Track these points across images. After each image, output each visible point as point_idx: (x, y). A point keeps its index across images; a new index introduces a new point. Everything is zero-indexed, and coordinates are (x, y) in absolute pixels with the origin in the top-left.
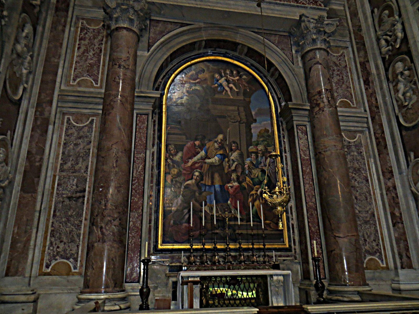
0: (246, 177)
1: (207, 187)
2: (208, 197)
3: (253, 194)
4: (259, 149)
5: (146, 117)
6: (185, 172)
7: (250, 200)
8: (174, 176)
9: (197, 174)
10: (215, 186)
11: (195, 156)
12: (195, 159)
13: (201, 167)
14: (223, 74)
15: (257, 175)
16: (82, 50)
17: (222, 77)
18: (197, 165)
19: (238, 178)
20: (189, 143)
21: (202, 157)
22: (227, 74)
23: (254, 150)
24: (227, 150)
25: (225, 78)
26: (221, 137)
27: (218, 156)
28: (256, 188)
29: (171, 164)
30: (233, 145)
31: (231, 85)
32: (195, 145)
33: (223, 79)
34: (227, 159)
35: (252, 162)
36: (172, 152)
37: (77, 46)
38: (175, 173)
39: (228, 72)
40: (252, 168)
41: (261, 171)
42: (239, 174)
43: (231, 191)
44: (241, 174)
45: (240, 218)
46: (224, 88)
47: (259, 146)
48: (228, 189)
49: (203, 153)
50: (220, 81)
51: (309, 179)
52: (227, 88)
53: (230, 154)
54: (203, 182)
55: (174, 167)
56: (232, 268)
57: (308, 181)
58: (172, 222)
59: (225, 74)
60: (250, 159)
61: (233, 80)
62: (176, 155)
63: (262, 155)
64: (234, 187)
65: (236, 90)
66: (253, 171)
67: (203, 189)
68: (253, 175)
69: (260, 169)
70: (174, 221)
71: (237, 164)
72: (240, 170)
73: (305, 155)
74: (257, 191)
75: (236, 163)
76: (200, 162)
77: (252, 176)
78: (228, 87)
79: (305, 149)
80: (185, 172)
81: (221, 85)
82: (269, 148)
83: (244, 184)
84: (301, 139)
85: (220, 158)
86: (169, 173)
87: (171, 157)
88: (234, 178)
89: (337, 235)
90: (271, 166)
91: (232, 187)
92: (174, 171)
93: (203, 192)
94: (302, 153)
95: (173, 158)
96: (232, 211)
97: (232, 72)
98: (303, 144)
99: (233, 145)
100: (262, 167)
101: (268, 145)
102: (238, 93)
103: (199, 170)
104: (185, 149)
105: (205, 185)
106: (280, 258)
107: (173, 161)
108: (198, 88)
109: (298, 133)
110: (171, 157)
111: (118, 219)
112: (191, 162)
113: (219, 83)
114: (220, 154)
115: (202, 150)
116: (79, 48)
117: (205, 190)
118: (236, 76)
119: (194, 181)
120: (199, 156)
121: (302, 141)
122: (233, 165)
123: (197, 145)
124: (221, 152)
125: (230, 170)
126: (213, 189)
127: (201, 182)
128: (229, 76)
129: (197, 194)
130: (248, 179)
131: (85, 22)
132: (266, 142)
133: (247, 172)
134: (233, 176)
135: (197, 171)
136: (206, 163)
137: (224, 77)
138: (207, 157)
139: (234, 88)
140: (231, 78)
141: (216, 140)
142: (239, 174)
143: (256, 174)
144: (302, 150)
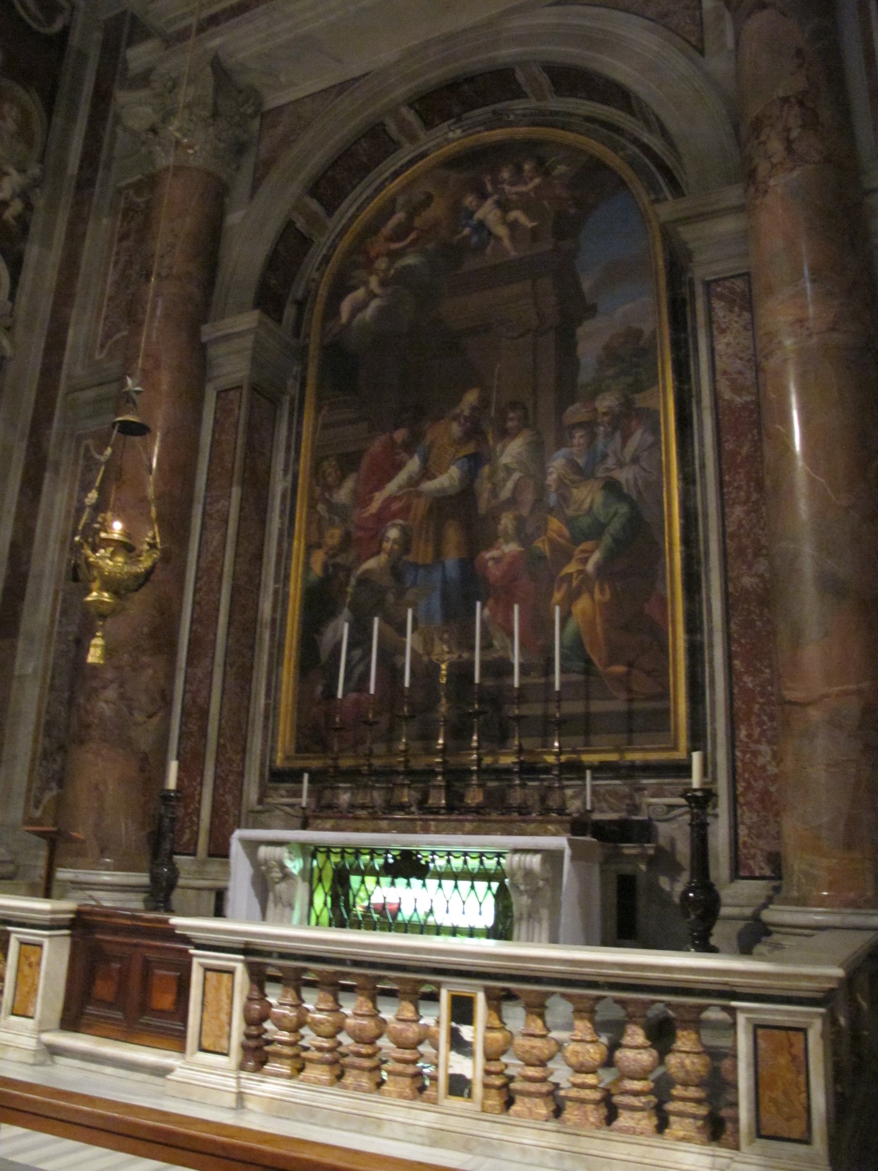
0: (549, 516)
5: (238, 394)
6: (361, 534)
7: (558, 596)
9: (393, 533)
10: (443, 566)
11: (390, 478)
12: (392, 487)
13: (405, 512)
14: (489, 188)
15: (586, 505)
16: (120, 266)
17: (483, 196)
18: (395, 506)
19: (520, 522)
21: (410, 478)
22: (503, 182)
25: (496, 197)
26: (471, 397)
27: (459, 463)
28: (583, 551)
29: (326, 515)
30: (511, 415)
33: (489, 203)
34: (486, 470)
35: (571, 463)
36: (330, 479)
37: (113, 259)
40: (573, 482)
42: (525, 511)
43: (494, 571)
44: (532, 512)
45: (521, 665)
46: (490, 233)
47: (600, 397)
49: (413, 465)
50: (479, 215)
52: (501, 231)
53: (498, 449)
54: (410, 558)
55: (332, 524)
56: (436, 827)
57: (742, 494)
58: (319, 689)
59: (496, 182)
60: (564, 451)
65: (530, 224)
66: (575, 491)
67: (409, 578)
71: (521, 478)
72: (528, 497)
73: (737, 389)
74: (585, 561)
75: (516, 476)
77: (570, 512)
79: (739, 365)
80: (361, 534)
81: (481, 226)
82: (637, 396)
84: (723, 331)
85: (466, 468)
86: (319, 546)
87: (327, 495)
88: (506, 528)
89: (790, 695)
92: (332, 537)
93: (407, 589)
95: (331, 496)
96: (496, 643)
97: (519, 169)
98: (730, 351)
100: (608, 470)
101: (638, 387)
102: (535, 235)
103: (400, 522)
104: (365, 462)
105: (416, 566)
107: (332, 507)
108: (410, 260)
109: (710, 310)
110: (327, 495)
111: (115, 686)
112: (379, 498)
113: (474, 221)
114: (465, 456)
115: (411, 456)
116: (116, 263)
117: (414, 584)
118: (531, 179)
119: (383, 558)
120: (402, 477)
121: (728, 338)
122: (505, 480)
124: (470, 448)
126: (437, 575)
127: (405, 558)
128: (507, 188)
129: (390, 598)
130: (555, 524)
131: (131, 192)
135: (394, 525)
136: (419, 494)
137: (491, 195)
138: (426, 473)
141: (457, 411)
142: (525, 511)
143: (583, 501)
144: (725, 373)
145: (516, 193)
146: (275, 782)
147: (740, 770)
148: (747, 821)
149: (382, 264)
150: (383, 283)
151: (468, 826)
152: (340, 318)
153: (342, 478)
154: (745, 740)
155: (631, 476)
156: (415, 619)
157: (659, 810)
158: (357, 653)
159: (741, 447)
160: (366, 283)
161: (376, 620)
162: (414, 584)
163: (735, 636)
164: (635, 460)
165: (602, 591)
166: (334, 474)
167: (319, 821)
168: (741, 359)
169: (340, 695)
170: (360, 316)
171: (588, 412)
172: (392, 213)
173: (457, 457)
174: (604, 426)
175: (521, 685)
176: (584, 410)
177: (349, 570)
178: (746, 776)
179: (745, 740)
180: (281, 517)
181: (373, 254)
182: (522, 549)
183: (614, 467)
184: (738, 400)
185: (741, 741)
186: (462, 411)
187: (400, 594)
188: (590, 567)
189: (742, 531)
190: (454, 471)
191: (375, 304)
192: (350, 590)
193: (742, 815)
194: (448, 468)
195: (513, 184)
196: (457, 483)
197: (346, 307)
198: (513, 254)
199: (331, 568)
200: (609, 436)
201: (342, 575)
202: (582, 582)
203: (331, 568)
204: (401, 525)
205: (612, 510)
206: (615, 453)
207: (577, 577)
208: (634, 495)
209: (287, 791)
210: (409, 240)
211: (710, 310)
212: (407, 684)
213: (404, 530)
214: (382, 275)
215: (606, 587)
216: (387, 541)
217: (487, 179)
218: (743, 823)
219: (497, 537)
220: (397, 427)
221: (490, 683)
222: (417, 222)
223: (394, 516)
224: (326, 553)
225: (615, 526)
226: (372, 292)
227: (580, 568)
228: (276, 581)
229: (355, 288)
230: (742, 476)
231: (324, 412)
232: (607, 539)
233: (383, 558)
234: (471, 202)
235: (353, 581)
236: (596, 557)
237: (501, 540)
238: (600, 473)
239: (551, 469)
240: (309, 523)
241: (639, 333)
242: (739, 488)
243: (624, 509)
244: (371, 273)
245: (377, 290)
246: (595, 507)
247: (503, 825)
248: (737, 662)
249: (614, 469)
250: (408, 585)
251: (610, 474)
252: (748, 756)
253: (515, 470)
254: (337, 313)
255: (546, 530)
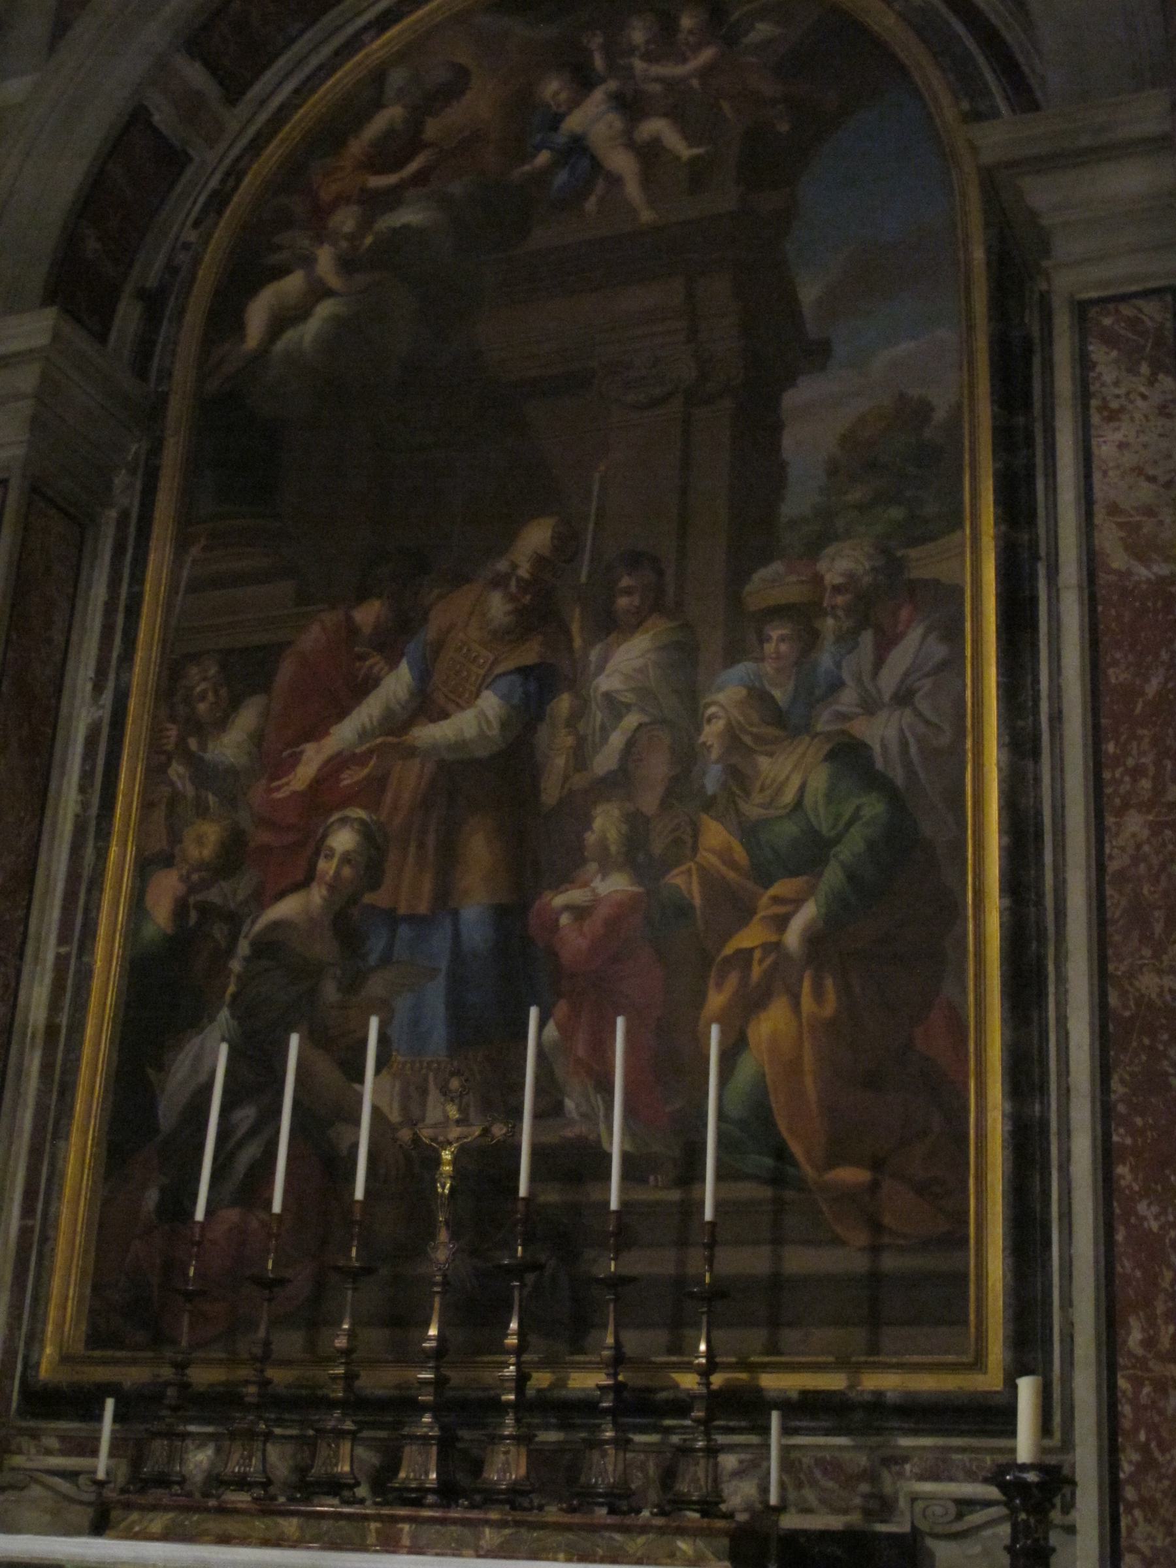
0: (704, 817)
1: (404, 931)
2: (403, 1004)
3: (751, 951)
4: (832, 578)
7: (716, 1000)
8: (195, 877)
9: (343, 840)
11: (342, 714)
14: (599, 62)
15: (789, 796)
17: (584, 81)
18: (349, 779)
20: (315, 630)
22: (632, 50)
23: (791, 591)
24: (575, 628)
25: (612, 85)
27: (503, 684)
28: (776, 900)
29: (190, 791)
30: (625, 582)
31: (656, 127)
32: (353, 630)
33: (598, 94)
34: (564, 703)
35: (758, 696)
36: (202, 707)
38: (207, 853)
39: (638, 34)
40: (757, 738)
41: (831, 756)
45: (626, 1157)
46: (596, 165)
47: (830, 550)
48: (555, 927)
50: (574, 122)
51: (1158, 763)
52: (622, 162)
54: (378, 898)
55: (202, 810)
56: (414, 1537)
57: (1146, 784)
58: (152, 1197)
60: (743, 669)
61: (670, 84)
62: (222, 724)
63: (848, 624)
64: (603, 912)
65: (685, 152)
66: (764, 762)
67: (376, 946)
68: (757, 798)
69: (828, 736)
70: (163, 1190)
73: (1140, 551)
74: (781, 923)
75: (632, 720)
76: (371, 751)
77: (752, 810)
78: (630, 144)
79: (1145, 492)
80: (264, 837)
81: (578, 146)
82: (913, 553)
83: (677, 879)
84: (1113, 416)
86: (167, 860)
87: (193, 743)
88: (603, 844)
90: (924, 706)
91: (580, 913)
92: (200, 841)
94: (1109, 538)
95: (203, 746)
96: (569, 1104)
97: (667, 26)
98: (1129, 459)
99: (625, 582)
100: (843, 717)
103: (361, 813)
104: (286, 670)
105: (392, 918)
106: (928, 1487)
107: (202, 772)
108: (409, 216)
113: (561, 138)
115: (393, 664)
118: (697, 48)
119: (316, 895)
120: (369, 711)
121: (1124, 431)
122: (605, 731)
123: (367, 630)
124: (530, 654)
125: (579, 781)
126: (440, 941)
127: (368, 898)
128: (639, 65)
129: (330, 991)
132: (896, 513)
133: (712, 779)
134: (598, 824)
135: (344, 821)
136: (411, 752)
137: (603, 80)
139: (673, 139)
140: (657, 70)
141: (502, 566)
142: (649, 802)
143: (779, 791)
144: (1114, 509)
145: (658, 79)
146: (35, 1416)
147: (1126, 1424)
148: (1141, 1545)
149: (345, 220)
150: (347, 265)
151: (489, 1536)
152: (243, 338)
153: (235, 703)
154: (1140, 1351)
155: (892, 733)
156: (383, 1039)
157: (939, 1510)
158: (246, 1115)
159: (1147, 680)
160: (308, 262)
161: (294, 1040)
162: (386, 959)
163: (1122, 1108)
164: (904, 697)
165: (818, 993)
166: (211, 697)
167: (135, 1516)
168: (1152, 479)
169: (200, 1215)
170: (290, 335)
171: (802, 582)
172: (378, 105)
173: (499, 670)
174: (836, 617)
175: (624, 1203)
176: (793, 578)
177: (234, 921)
178: (1142, 1437)
179: (1140, 1351)
180: (82, 789)
181: (326, 194)
182: (636, 889)
183: (858, 710)
184: (1142, 572)
185: (1130, 1354)
186: (514, 566)
187: (352, 984)
188: (793, 937)
189: (1142, 867)
190: (490, 703)
191: (325, 309)
192: (236, 966)
193: (1130, 1530)
194: (477, 695)
195: (648, 57)
196: (495, 732)
197: (257, 315)
198: (647, 216)
199: (193, 916)
200: (848, 639)
201: (219, 931)
202: (775, 966)
203: (193, 916)
204: (362, 822)
205: (848, 811)
206: (859, 681)
207: (761, 961)
208: (898, 776)
209: (62, 1438)
210: (413, 167)
211: (1083, 363)
212: (359, 1194)
213: (367, 833)
214: (344, 244)
215: (829, 983)
216: (330, 856)
217: (596, 42)
218: (1133, 1549)
219: (584, 861)
220: (362, 596)
221: (552, 1196)
222: (432, 129)
223: (348, 800)
224: (185, 879)
225: (851, 847)
226: (320, 281)
227: (774, 938)
228: (63, 939)
229: (281, 272)
230: (1145, 745)
231: (195, 551)
232: (833, 876)
233: (316, 895)
234: (556, 93)
235: (244, 947)
236: (808, 913)
237: (593, 867)
238: (824, 723)
239: (713, 710)
240: (148, 805)
241: (924, 409)
242: (1137, 772)
243: (874, 807)
244: (319, 239)
245: (334, 281)
246: (808, 801)
247: (570, 1536)
248: (1122, 1170)
249: (857, 715)
250: (373, 959)
251: (846, 726)
252: (1146, 1390)
253: (628, 707)
254: (238, 327)
255: (695, 849)
